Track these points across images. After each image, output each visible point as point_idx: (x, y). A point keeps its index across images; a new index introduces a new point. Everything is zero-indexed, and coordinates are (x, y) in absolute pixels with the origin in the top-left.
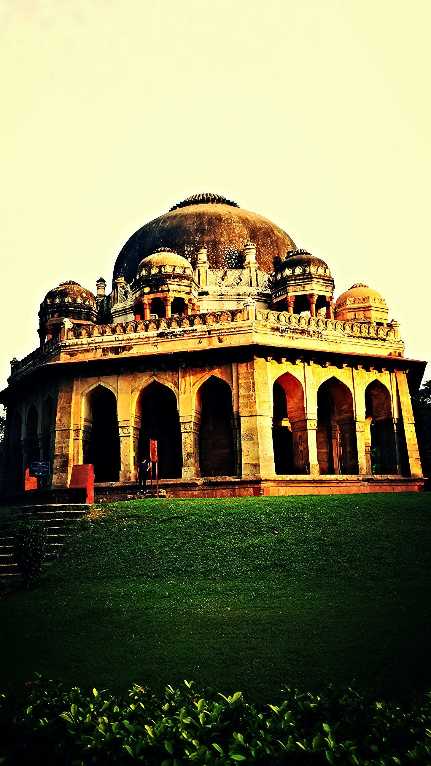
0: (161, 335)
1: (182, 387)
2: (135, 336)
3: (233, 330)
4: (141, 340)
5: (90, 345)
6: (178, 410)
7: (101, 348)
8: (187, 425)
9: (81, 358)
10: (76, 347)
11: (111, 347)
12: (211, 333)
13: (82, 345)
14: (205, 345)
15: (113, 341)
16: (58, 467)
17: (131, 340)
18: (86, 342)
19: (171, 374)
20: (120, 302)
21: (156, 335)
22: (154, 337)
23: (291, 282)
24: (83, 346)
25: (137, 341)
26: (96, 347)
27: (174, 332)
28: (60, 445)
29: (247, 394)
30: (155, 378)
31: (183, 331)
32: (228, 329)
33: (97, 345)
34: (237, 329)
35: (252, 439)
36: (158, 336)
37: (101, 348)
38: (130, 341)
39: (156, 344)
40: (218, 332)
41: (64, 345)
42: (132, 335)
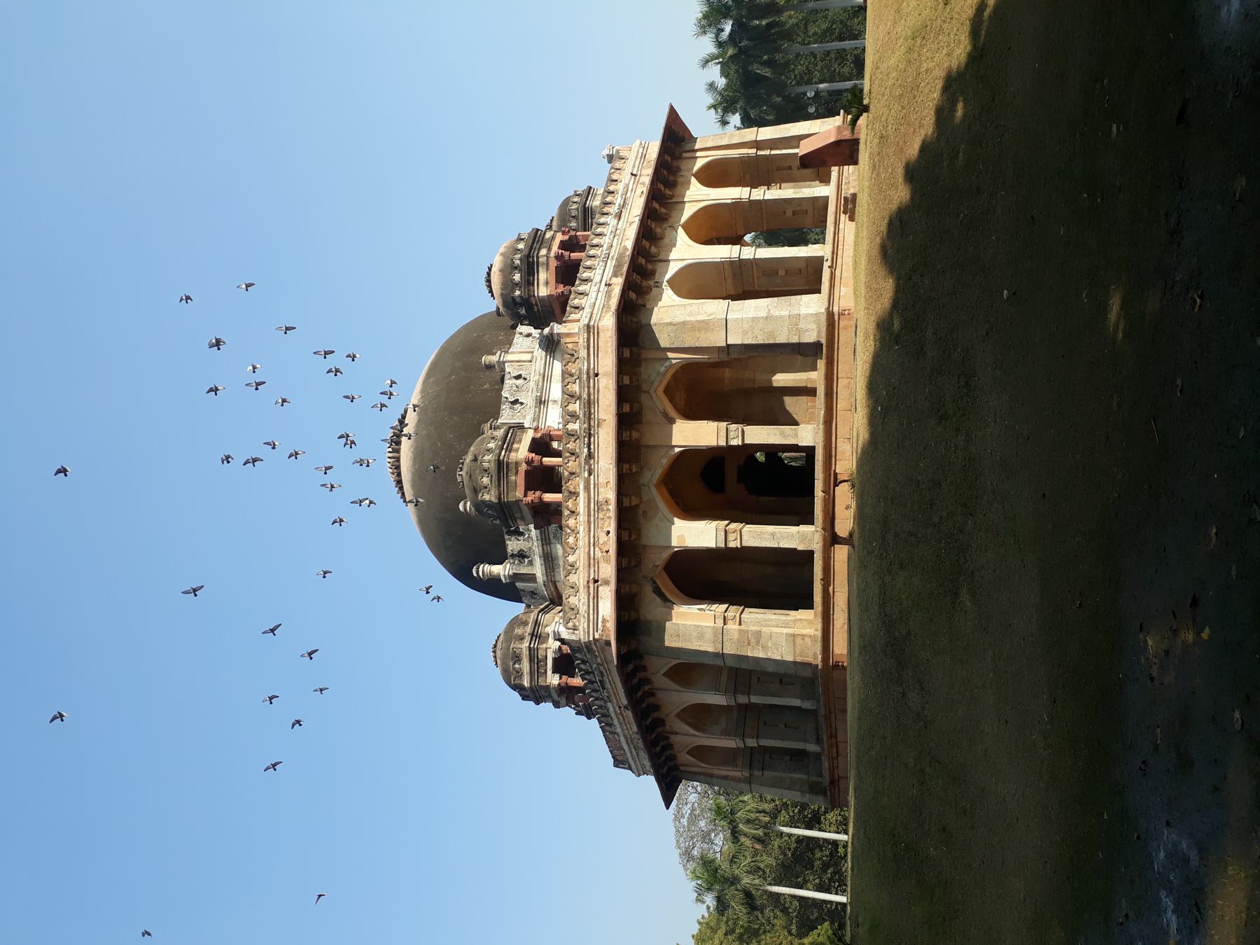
0: (619, 216)
4: (616, 237)
5: (602, 289)
6: (729, 201)
7: (610, 279)
10: (597, 306)
12: (634, 173)
14: (647, 180)
23: (588, 203)
26: (606, 285)
27: (620, 204)
29: (727, 138)
33: (603, 283)
36: (619, 220)
37: (610, 279)
38: (614, 248)
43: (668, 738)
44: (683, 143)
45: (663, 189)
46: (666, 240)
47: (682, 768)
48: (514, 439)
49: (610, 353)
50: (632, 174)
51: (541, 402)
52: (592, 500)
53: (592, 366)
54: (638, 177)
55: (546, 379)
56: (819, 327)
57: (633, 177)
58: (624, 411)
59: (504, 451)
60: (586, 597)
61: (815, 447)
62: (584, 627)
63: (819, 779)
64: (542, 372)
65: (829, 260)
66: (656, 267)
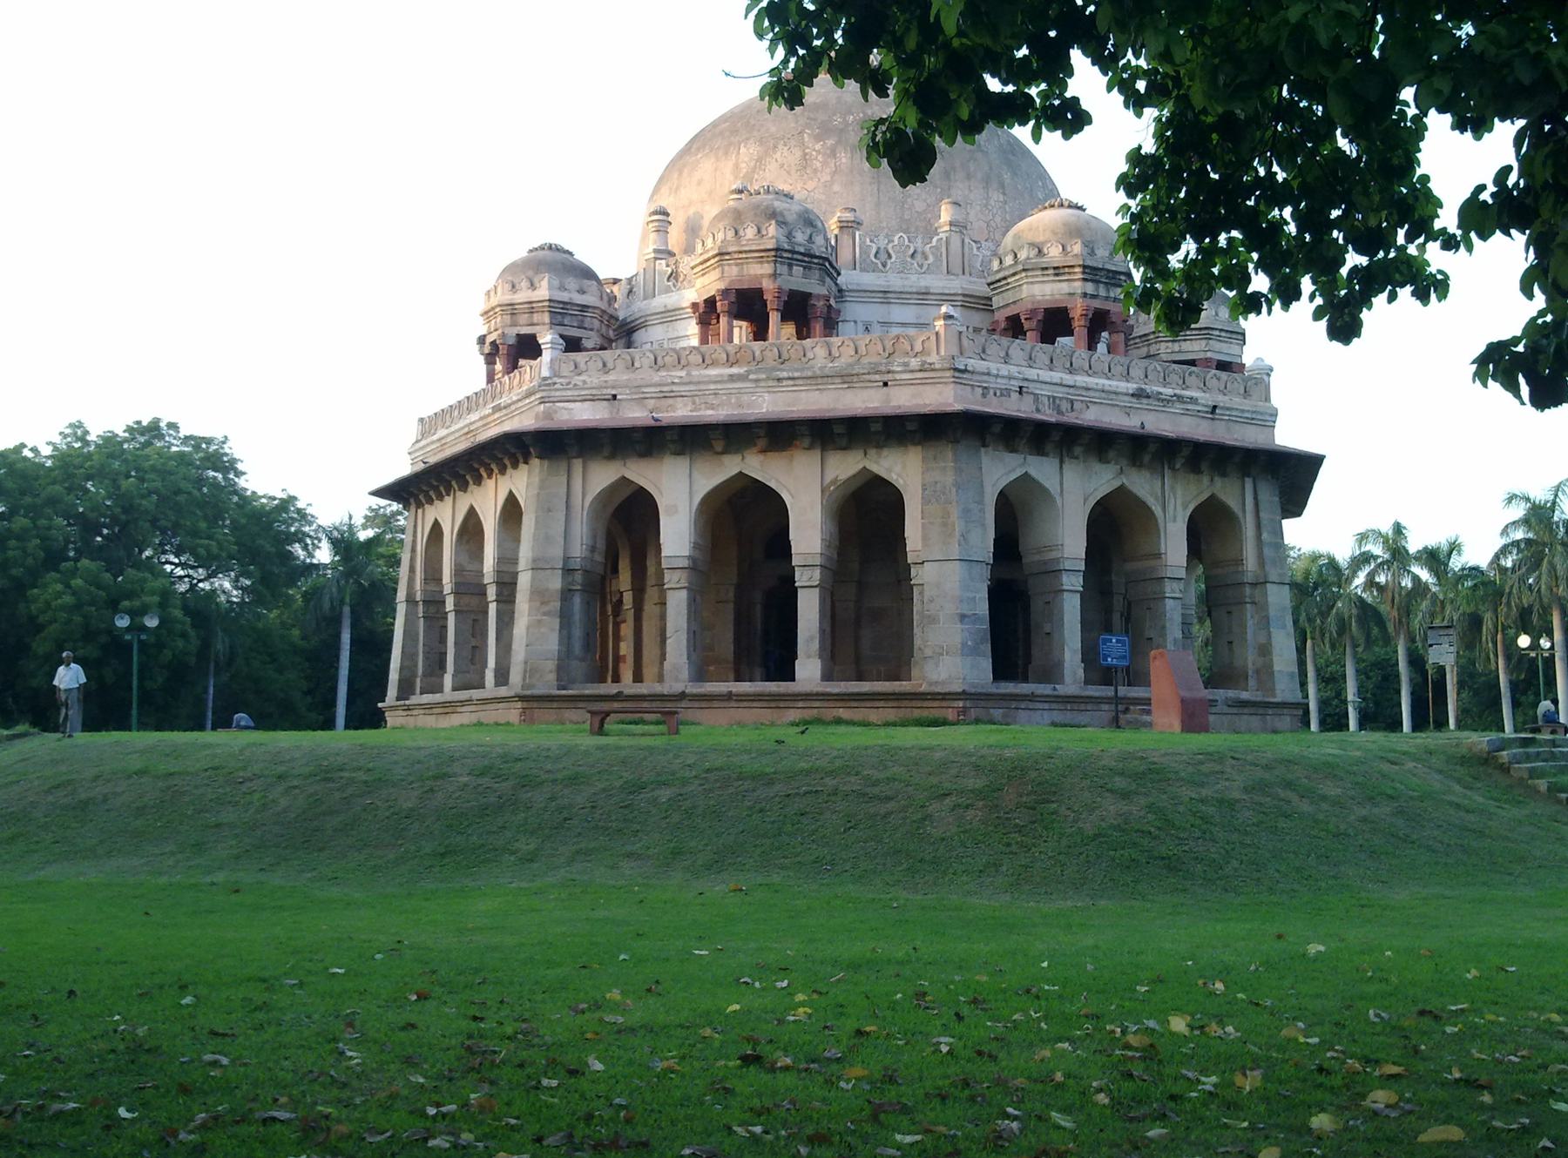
1: (1170, 508)
2: (1097, 384)
3: (1249, 416)
4: (1103, 395)
5: (1013, 382)
8: (1175, 585)
9: (993, 407)
10: (985, 378)
11: (1049, 397)
13: (997, 376)
15: (1056, 384)
16: (969, 643)
17: (1088, 389)
18: (1006, 373)
19: (1148, 475)
20: (862, 270)
21: (1131, 392)
22: (1127, 394)
24: (999, 380)
25: (1097, 394)
26: (1021, 388)
27: (1161, 394)
28: (971, 595)
30: (1125, 481)
31: (1175, 395)
32: (1243, 411)
34: (1254, 416)
35: (1284, 627)
36: (1133, 395)
39: (1128, 410)
40: (1228, 413)
41: (963, 368)
42: (1092, 381)
43: (448, 495)
44: (1269, 477)
45: (1182, 454)
46: (1097, 467)
47: (420, 511)
48: (810, 268)
49: (914, 402)
50: (1215, 407)
51: (885, 296)
52: (719, 386)
53: (898, 377)
54: (1210, 416)
55: (921, 297)
56: (943, 683)
57: (1210, 410)
58: (834, 427)
59: (790, 256)
60: (594, 385)
61: (794, 680)
62: (555, 384)
63: (418, 691)
64: (931, 291)
65: (1056, 693)
66: (1052, 455)
